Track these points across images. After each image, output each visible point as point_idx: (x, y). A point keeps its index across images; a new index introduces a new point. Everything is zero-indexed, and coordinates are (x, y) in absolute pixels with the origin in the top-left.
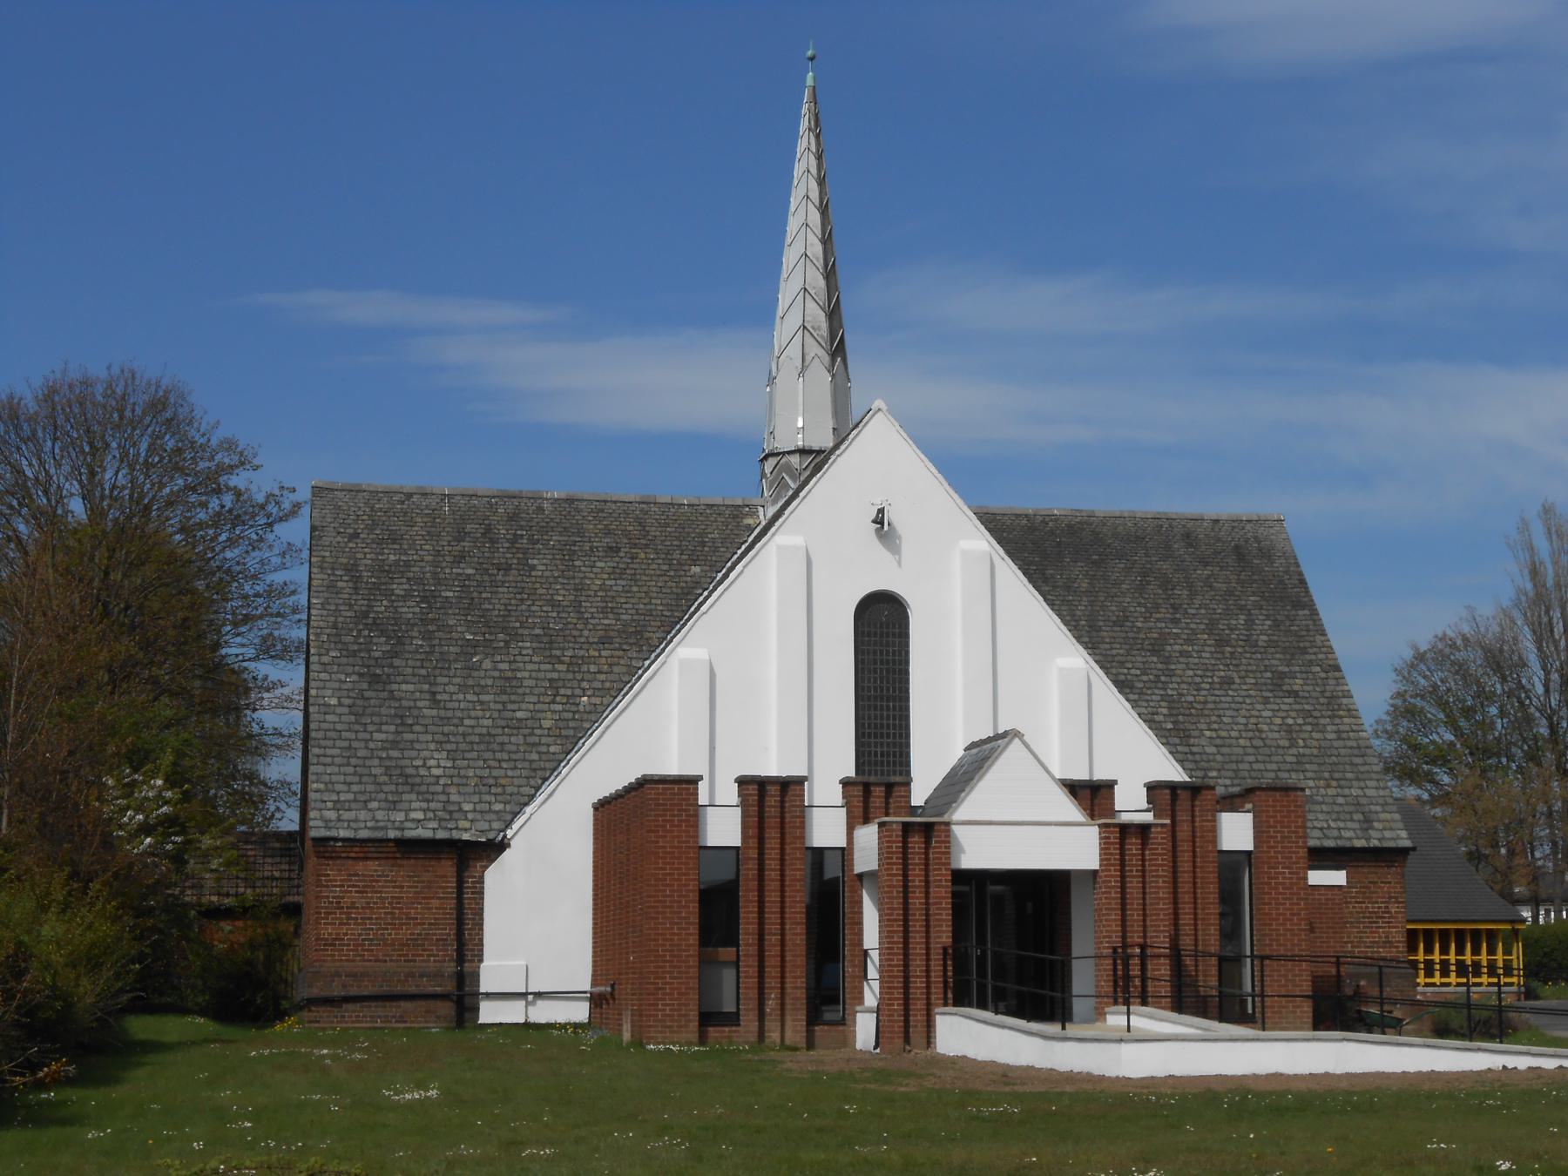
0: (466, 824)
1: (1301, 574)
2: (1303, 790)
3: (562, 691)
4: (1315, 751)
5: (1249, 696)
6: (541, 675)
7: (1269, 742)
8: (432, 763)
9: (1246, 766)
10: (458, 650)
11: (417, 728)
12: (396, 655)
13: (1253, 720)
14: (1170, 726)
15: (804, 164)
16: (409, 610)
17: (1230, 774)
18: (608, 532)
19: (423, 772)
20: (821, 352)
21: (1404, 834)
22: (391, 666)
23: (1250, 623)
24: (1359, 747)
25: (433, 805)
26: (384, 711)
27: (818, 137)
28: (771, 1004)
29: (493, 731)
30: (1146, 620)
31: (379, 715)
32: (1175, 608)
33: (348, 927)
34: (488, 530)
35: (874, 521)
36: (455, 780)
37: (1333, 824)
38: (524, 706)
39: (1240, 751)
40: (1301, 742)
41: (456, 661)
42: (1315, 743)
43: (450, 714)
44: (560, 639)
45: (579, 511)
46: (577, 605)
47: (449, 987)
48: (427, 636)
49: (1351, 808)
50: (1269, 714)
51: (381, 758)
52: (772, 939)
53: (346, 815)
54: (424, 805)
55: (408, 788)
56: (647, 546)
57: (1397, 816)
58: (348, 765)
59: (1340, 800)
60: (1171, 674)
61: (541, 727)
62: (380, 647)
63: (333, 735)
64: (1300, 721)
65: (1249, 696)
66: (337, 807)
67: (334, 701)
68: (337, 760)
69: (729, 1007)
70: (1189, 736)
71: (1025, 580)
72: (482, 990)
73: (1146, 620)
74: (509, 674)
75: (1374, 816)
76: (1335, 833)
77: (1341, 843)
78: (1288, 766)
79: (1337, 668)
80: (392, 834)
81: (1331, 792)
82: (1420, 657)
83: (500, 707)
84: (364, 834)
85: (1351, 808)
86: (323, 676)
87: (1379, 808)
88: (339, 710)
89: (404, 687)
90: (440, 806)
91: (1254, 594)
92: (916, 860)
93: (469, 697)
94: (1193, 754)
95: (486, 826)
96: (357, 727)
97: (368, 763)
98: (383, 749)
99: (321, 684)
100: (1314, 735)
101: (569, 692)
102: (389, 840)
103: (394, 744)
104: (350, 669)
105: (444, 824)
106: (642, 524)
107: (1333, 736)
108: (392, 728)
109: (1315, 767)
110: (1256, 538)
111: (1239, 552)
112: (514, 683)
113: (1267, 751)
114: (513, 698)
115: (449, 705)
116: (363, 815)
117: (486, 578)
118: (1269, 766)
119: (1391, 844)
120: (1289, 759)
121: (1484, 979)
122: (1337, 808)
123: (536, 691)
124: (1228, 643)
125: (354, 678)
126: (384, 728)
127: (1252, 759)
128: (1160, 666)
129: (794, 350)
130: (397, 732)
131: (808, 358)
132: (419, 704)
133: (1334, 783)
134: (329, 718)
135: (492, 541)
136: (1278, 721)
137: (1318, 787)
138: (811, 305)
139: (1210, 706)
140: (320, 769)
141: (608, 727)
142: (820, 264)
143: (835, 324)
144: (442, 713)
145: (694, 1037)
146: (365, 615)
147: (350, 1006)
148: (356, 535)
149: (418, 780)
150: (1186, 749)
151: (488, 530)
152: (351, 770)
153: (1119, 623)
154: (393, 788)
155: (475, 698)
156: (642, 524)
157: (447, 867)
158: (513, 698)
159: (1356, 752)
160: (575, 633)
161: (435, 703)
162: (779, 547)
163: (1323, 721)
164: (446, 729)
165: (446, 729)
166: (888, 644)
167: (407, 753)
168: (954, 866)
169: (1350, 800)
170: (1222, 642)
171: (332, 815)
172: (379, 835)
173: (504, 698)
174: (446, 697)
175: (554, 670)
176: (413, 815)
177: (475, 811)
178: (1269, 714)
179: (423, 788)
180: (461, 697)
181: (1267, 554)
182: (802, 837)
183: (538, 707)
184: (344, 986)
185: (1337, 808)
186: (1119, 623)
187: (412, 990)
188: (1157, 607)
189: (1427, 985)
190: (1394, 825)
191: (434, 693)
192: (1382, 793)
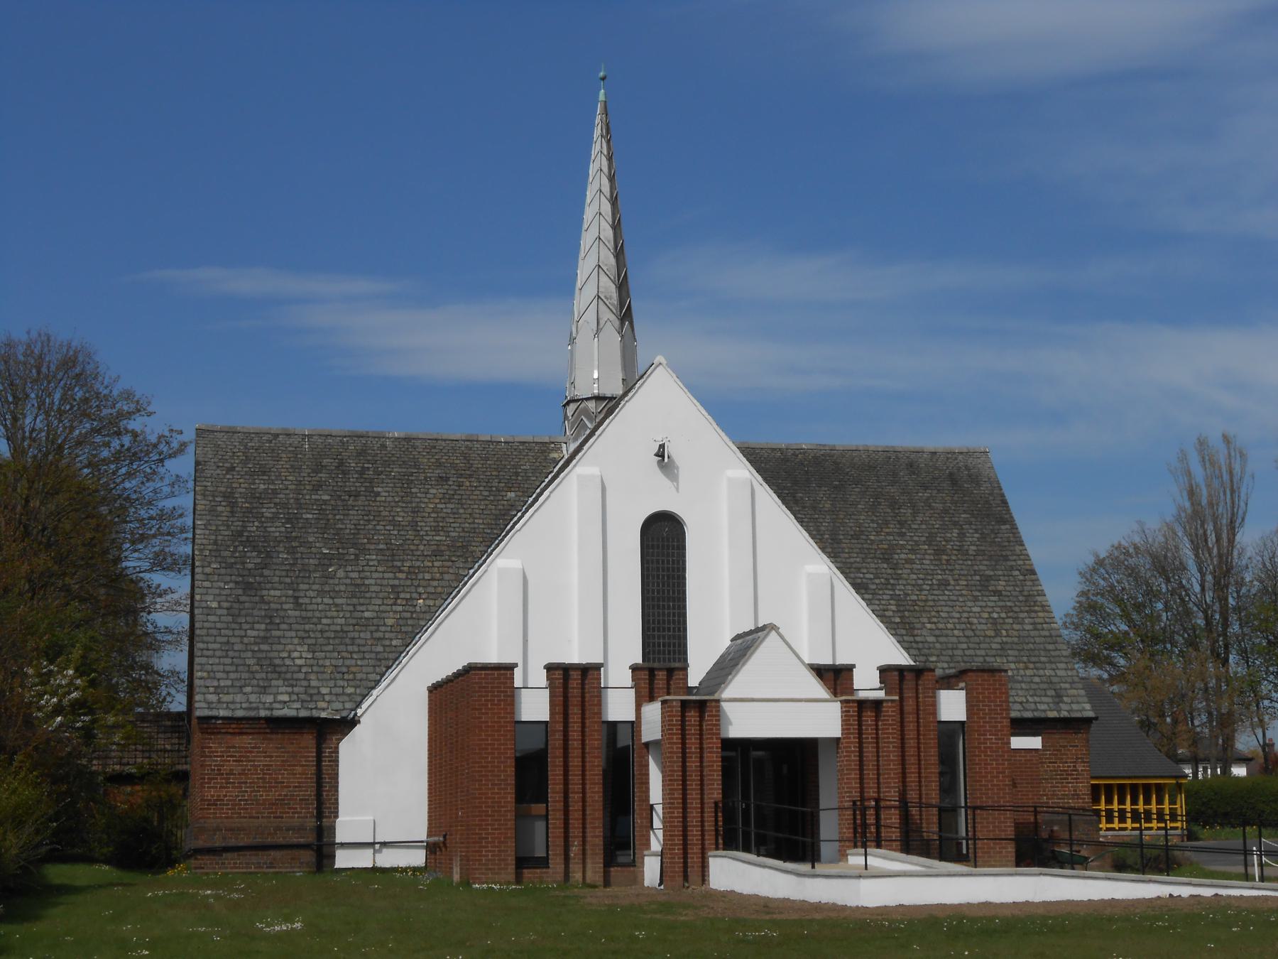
0: (324, 705)
1: (1003, 495)
2: (1006, 671)
3: (402, 595)
4: (1016, 640)
5: (962, 595)
6: (385, 582)
7: (978, 633)
8: (296, 654)
10: (316, 562)
11: (283, 626)
12: (265, 566)
13: (965, 615)
14: (898, 620)
15: (598, 164)
16: (276, 530)
17: (947, 659)
18: (439, 464)
19: (288, 662)
20: (613, 317)
21: (1088, 706)
22: (262, 575)
23: (962, 535)
24: (1051, 636)
25: (296, 689)
26: (256, 612)
27: (608, 142)
28: (575, 850)
29: (345, 628)
30: (878, 533)
31: (252, 615)
32: (902, 523)
33: (227, 790)
34: (341, 463)
35: (657, 455)
36: (315, 669)
37: (1030, 699)
38: (370, 608)
39: (954, 640)
40: (1004, 633)
41: (315, 571)
42: (1015, 633)
43: (310, 614)
44: (400, 552)
45: (414, 447)
46: (414, 525)
47: (311, 838)
48: (292, 551)
49: (1045, 686)
50: (978, 609)
51: (253, 651)
52: (575, 797)
53: (225, 698)
54: (290, 689)
55: (275, 676)
56: (471, 476)
57: (1082, 692)
58: (227, 656)
59: (1037, 679)
60: (899, 577)
61: (385, 625)
62: (253, 560)
63: (214, 632)
64: (1003, 615)
65: (962, 595)
66: (218, 690)
67: (214, 605)
68: (218, 653)
69: (540, 853)
70: (914, 629)
71: (779, 502)
72: (338, 840)
73: (878, 533)
74: (359, 582)
75: (1063, 692)
76: (1033, 706)
77: (1037, 714)
78: (994, 652)
79: (1033, 572)
80: (263, 713)
81: (1029, 672)
82: (1100, 562)
83: (351, 608)
84: (240, 713)
85: (1045, 686)
86: (207, 584)
87: (1067, 686)
88: (219, 612)
89: (272, 593)
90: (302, 690)
91: (965, 512)
92: (692, 730)
93: (326, 600)
94: (917, 642)
95: (340, 706)
96: (234, 626)
97: (243, 655)
98: (255, 643)
99: (204, 591)
100: (1015, 626)
101: (408, 596)
102: (260, 719)
103: (265, 639)
104: (228, 578)
105: (305, 705)
106: (466, 457)
107: (1030, 627)
108: (263, 627)
109: (1016, 653)
110: (967, 468)
111: (953, 479)
112: (363, 588)
113: (977, 640)
114: (362, 601)
115: (310, 607)
116: (239, 698)
117: (339, 503)
118: (978, 652)
119: (1078, 715)
120: (994, 646)
121: (1154, 824)
123: (381, 595)
124: (943, 552)
125: (231, 585)
126: (256, 626)
127: (965, 646)
128: (889, 571)
129: (591, 316)
130: (266, 630)
131: (602, 323)
132: (286, 606)
133: (1031, 666)
134: (211, 618)
135: (344, 473)
136: (986, 615)
137: (1018, 669)
138: (604, 279)
139: (931, 603)
140: (203, 660)
141: (440, 624)
142: (611, 246)
143: (624, 294)
144: (304, 614)
145: (512, 877)
146: (240, 534)
147: (229, 855)
148: (233, 469)
149: (284, 669)
150: (911, 639)
151: (341, 463)
152: (228, 661)
153: (856, 536)
154: (264, 675)
155: (331, 601)
156: (466, 457)
157: (308, 740)
158: (362, 601)
159: (1049, 640)
160: (412, 547)
161: (298, 605)
162: (579, 476)
163: (1022, 615)
164: (307, 627)
165: (307, 627)
166: (668, 555)
167: (275, 647)
168: (723, 735)
169: (1044, 679)
170: (939, 552)
171: (213, 698)
172: (252, 714)
173: (355, 601)
174: (307, 600)
175: (395, 578)
176: (281, 698)
177: (331, 693)
178: (978, 609)
179: (289, 676)
180: (319, 600)
181: (975, 479)
182: (599, 713)
183: (382, 608)
184: (224, 838)
185: (1034, 686)
186: (856, 536)
187: (280, 841)
188: (887, 523)
189: (1108, 829)
190: (1080, 699)
191: (297, 598)
192: (1070, 673)
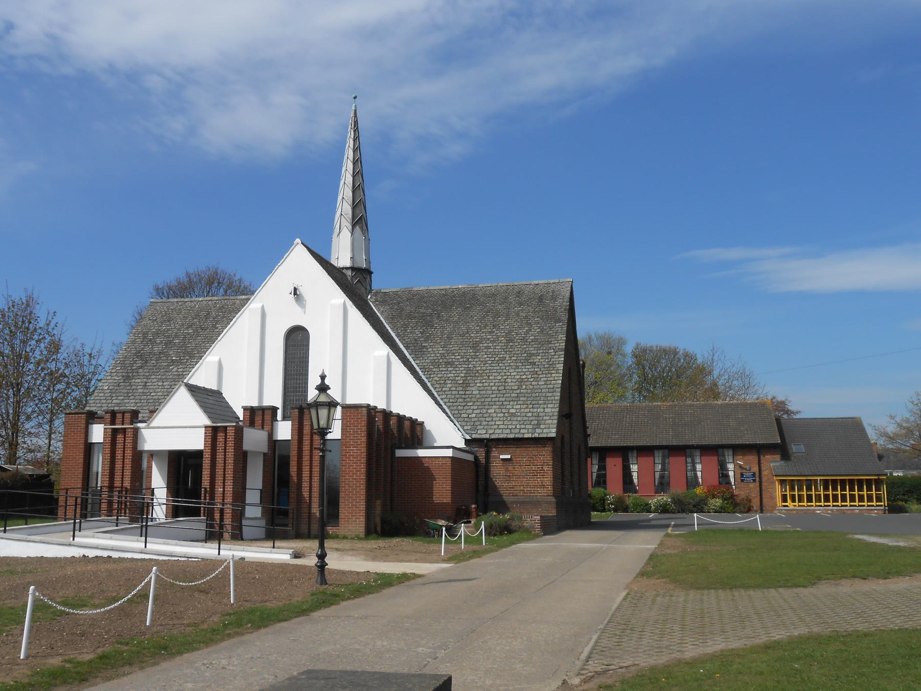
9: (489, 399)
12: (141, 367)
32: (494, 326)
39: (490, 392)
110: (553, 292)
111: (541, 299)
122: (525, 418)
143: (357, 211)
153: (462, 335)
170: (509, 341)
185: (525, 418)
186: (462, 335)
